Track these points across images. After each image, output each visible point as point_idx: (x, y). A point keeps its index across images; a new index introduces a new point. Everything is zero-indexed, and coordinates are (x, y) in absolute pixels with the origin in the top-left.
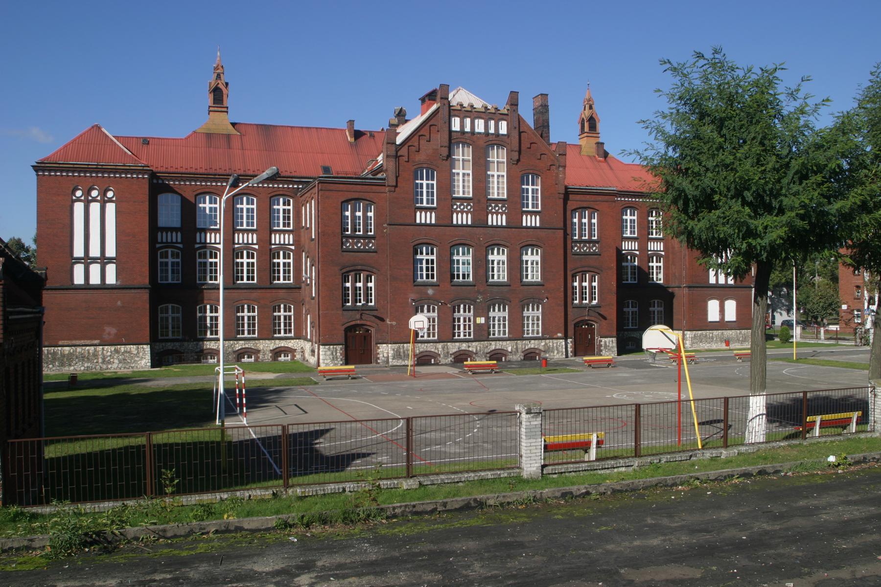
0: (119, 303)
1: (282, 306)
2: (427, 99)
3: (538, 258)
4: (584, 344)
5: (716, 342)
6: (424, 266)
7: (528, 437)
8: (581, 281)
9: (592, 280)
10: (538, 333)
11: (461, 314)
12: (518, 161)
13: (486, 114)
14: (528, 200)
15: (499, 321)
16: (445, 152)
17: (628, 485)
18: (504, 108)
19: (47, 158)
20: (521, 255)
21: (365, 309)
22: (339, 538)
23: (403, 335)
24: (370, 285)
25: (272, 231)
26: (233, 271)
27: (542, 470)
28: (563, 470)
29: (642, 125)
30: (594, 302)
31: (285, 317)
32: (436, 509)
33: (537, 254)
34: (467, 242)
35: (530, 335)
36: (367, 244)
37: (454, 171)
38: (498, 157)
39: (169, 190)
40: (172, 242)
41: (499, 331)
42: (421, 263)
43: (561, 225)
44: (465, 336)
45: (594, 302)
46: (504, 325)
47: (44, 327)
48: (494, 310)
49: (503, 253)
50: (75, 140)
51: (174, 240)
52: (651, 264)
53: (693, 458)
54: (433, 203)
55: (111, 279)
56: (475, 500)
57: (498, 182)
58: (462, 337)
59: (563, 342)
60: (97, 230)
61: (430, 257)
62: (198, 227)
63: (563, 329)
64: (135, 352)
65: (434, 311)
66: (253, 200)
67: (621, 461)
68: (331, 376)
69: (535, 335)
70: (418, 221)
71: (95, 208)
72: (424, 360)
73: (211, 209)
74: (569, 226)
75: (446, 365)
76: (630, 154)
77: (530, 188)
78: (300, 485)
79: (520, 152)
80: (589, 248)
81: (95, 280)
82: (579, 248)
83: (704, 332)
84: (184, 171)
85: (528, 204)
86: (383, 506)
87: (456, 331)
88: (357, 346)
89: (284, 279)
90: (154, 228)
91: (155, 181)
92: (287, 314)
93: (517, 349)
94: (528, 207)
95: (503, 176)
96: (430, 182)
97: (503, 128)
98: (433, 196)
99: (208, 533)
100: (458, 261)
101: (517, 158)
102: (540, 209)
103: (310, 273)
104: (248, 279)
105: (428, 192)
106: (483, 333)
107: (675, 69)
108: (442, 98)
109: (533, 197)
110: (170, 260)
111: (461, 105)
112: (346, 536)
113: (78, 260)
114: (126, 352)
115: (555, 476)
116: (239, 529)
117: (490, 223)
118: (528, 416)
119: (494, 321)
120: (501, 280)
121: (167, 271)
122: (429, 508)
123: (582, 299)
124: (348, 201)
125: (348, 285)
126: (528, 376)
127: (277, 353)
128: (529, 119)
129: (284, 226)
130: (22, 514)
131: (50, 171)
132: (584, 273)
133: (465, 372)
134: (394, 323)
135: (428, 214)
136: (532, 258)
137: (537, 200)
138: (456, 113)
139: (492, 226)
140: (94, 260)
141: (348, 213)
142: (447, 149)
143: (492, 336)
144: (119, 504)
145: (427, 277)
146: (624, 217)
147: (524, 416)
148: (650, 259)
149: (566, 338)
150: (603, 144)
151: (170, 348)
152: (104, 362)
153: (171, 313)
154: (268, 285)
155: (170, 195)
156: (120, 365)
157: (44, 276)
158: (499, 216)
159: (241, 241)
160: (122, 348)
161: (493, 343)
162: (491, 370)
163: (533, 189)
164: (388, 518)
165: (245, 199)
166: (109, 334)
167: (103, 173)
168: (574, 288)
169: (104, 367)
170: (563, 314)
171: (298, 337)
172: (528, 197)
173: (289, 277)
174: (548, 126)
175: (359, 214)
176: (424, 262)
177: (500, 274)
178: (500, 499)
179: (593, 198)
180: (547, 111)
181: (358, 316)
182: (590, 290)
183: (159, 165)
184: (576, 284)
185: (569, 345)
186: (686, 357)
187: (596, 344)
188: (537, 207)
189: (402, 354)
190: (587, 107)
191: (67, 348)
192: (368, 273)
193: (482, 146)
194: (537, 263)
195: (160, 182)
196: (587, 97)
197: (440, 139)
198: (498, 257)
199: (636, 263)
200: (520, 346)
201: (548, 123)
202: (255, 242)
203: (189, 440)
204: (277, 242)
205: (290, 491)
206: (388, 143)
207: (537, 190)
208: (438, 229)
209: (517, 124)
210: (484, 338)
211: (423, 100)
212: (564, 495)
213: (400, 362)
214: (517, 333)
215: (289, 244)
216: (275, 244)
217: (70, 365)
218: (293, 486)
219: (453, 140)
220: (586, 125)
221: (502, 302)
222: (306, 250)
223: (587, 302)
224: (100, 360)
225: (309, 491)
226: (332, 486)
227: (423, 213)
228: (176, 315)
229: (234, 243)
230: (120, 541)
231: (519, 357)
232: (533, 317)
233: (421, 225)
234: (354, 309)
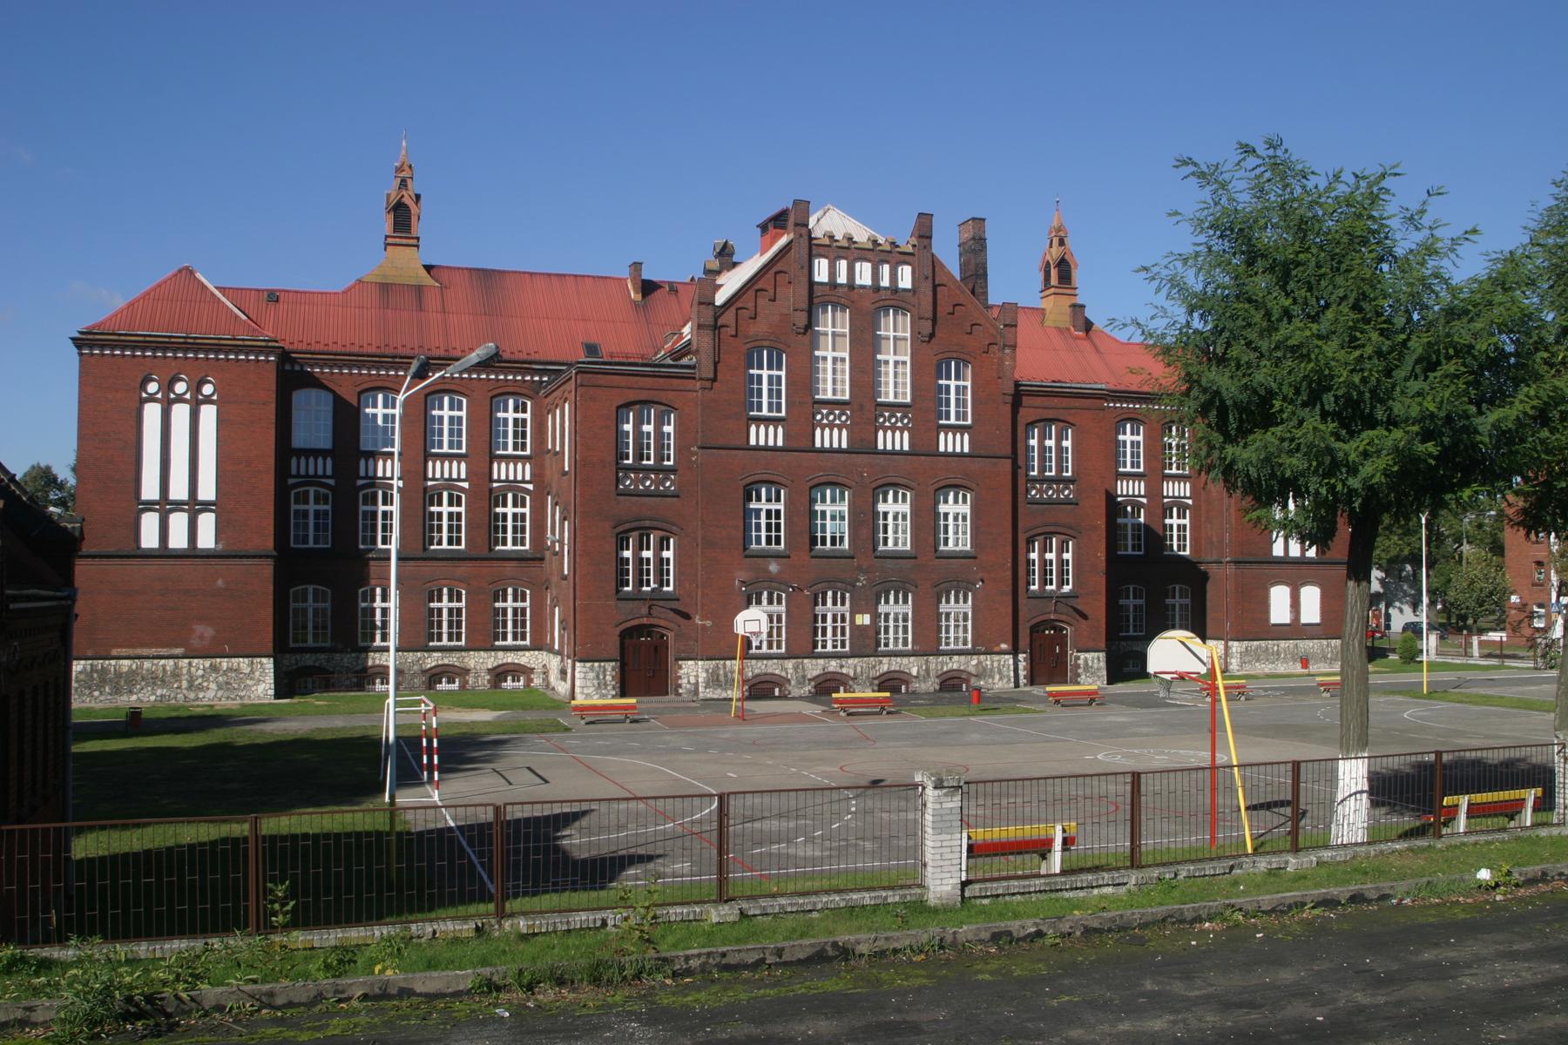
0: (220, 582)
1: (510, 591)
2: (770, 226)
3: (965, 509)
4: (1048, 664)
5: (1285, 661)
6: (763, 521)
7: (939, 830)
8: (1044, 550)
9: (1062, 549)
10: (965, 643)
11: (829, 608)
12: (932, 335)
13: (875, 254)
14: (948, 405)
15: (896, 620)
16: (801, 319)
17: (1113, 920)
18: (906, 242)
19: (99, 325)
20: (937, 503)
21: (657, 597)
22: (585, 1011)
23: (723, 645)
24: (665, 554)
25: (493, 457)
26: (421, 525)
27: (963, 891)
28: (1000, 891)
29: (1144, 274)
30: (1067, 589)
31: (515, 610)
32: (762, 960)
33: (965, 501)
34: (840, 480)
35: (952, 646)
36: (662, 483)
37: (817, 353)
38: (896, 330)
39: (314, 382)
40: (316, 476)
41: (896, 639)
42: (758, 517)
43: (1008, 450)
44: (835, 647)
45: (1067, 589)
46: (905, 628)
47: (77, 626)
48: (887, 602)
49: (904, 500)
50: (148, 293)
51: (320, 472)
52: (1168, 521)
53: (1237, 871)
54: (779, 410)
55: (207, 540)
56: (835, 945)
57: (896, 374)
58: (829, 648)
59: (1010, 659)
60: (184, 453)
61: (773, 506)
62: (363, 448)
64: (247, 671)
65: (779, 602)
66: (460, 402)
67: (1106, 875)
68: (595, 716)
69: (961, 647)
70: (753, 442)
71: (181, 413)
72: (761, 689)
73: (385, 417)
74: (1021, 451)
75: (800, 698)
76: (1125, 325)
77: (953, 383)
78: (524, 914)
79: (934, 321)
80: (1058, 491)
81: (178, 540)
82: (1040, 491)
83: (1263, 643)
84: (338, 349)
85: (948, 413)
86: (668, 955)
87: (820, 638)
88: (642, 664)
89: (515, 543)
90: (285, 450)
91: (288, 367)
92: (519, 604)
93: (927, 670)
94: (948, 418)
95: (904, 363)
96: (775, 373)
97: (906, 278)
98: (779, 396)
99: (349, 999)
100: (823, 513)
101: (930, 330)
102: (969, 422)
103: (560, 533)
104: (450, 542)
105: (770, 391)
106: (866, 643)
107: (1202, 175)
108: (796, 225)
109: (957, 400)
110: (312, 507)
111: (831, 237)
112: (597, 1008)
113: (149, 506)
114: (230, 669)
115: (986, 901)
116: (406, 993)
117: (880, 446)
118: (937, 792)
119: (886, 620)
120: (900, 547)
121: (306, 526)
122: (751, 958)
123: (1044, 582)
124: (628, 405)
125: (627, 554)
126: (948, 721)
127: (499, 674)
128: (951, 261)
129: (515, 448)
130: (23, 959)
131: (102, 347)
132: (1048, 535)
133: (834, 713)
134: (709, 623)
135: (771, 428)
136: (956, 509)
137: (965, 406)
138: (821, 250)
139: (885, 452)
140: (178, 506)
141: (628, 427)
142: (804, 315)
143: (882, 648)
144: (199, 944)
145: (769, 539)
146: (1121, 437)
147: (930, 793)
148: (1166, 511)
149: (1015, 651)
150: (1083, 306)
151: (310, 663)
152: (191, 687)
153: (312, 602)
154: (485, 553)
155: (313, 392)
156: (220, 693)
157: (77, 534)
158: (898, 434)
159: (438, 475)
160: (224, 663)
161: (885, 660)
162: (880, 708)
163: (958, 387)
164: (675, 975)
165: (446, 399)
166: (201, 637)
167: (196, 351)
168: (1029, 562)
169: (192, 695)
171: (537, 646)
172: (948, 400)
173: (523, 539)
174: (985, 275)
175: (648, 428)
176: (763, 515)
177: (898, 537)
178: (881, 944)
179: (1066, 402)
180: (984, 247)
181: (644, 611)
182: (1059, 566)
183: (295, 337)
184: (1034, 556)
185: (1022, 665)
186: (1226, 688)
187: (1070, 662)
188: (965, 419)
189: (722, 678)
190: (1056, 241)
191: (126, 662)
193: (868, 309)
194: (964, 519)
195: (297, 368)
196: (1055, 224)
197: (792, 296)
198: (895, 508)
199: (1142, 520)
200: (932, 666)
201: (985, 269)
202: (463, 476)
203: (137, 846)
204: (503, 477)
205: (507, 924)
206: (700, 303)
207: (965, 387)
209: (930, 272)
210: (868, 651)
211: (764, 227)
212: (996, 937)
213: (718, 694)
214: (928, 642)
215: (524, 481)
216: (499, 481)
217: (131, 692)
218: (512, 915)
219: (817, 298)
220: (1054, 273)
221: (902, 587)
222: (554, 491)
223: (1054, 587)
224: (185, 684)
225: (542, 924)
226: (583, 916)
227: (762, 428)
228: (321, 605)
229: (426, 479)
230: (190, 1011)
231: (931, 685)
232: (957, 614)
233: (757, 448)
234: (638, 597)
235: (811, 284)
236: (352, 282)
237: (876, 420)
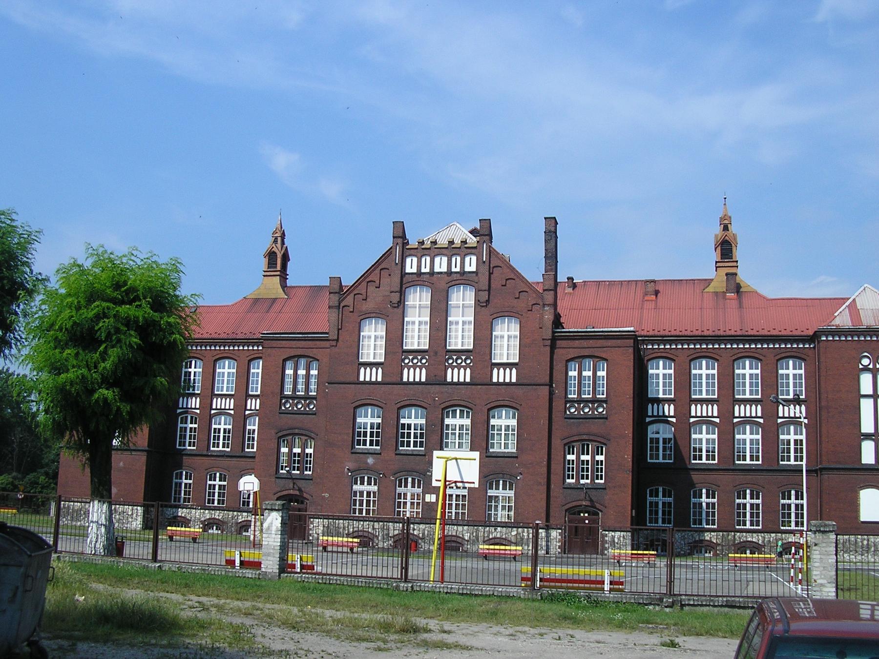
0: (121, 464)
12: (488, 301)
16: (395, 298)
36: (308, 405)
63: (544, 515)
97: (471, 264)
111: (451, 242)
117: (449, 379)
138: (412, 252)
139: (452, 383)
158: (462, 370)
159: (253, 408)
170: (545, 495)
179: (600, 343)
181: (291, 486)
182: (593, 466)
192: (304, 438)
200: (481, 534)
208: (383, 387)
235: (403, 274)
236: (242, 298)
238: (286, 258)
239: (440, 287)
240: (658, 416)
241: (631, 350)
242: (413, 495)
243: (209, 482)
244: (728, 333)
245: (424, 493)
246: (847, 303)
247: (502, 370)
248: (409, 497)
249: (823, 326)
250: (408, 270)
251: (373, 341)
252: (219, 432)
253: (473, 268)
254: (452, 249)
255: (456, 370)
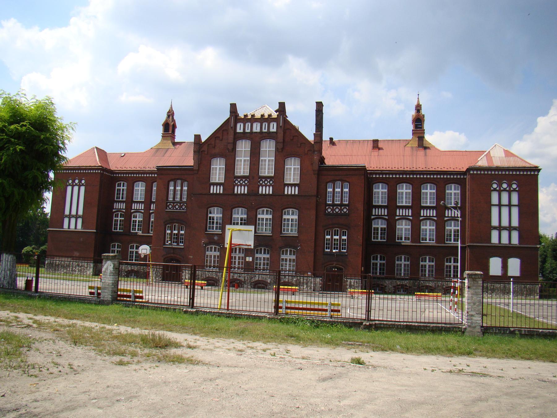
0: (81, 239)
12: (283, 149)
16: (230, 147)
71: (76, 188)
97: (273, 128)
110: (119, 219)
113: (66, 216)
161: (257, 276)
193: (256, 140)
235: (235, 133)
236: (150, 148)
237: (259, 182)
238: (174, 127)
239: (256, 140)
240: (378, 215)
241: (363, 177)
242: (239, 258)
243: (130, 250)
244: (418, 169)
245: (246, 256)
246: (486, 153)
247: (290, 188)
248: (237, 258)
249: (472, 165)
250: (238, 131)
251: (218, 171)
252: (136, 222)
253: (275, 130)
254: (262, 120)
255: (264, 188)
